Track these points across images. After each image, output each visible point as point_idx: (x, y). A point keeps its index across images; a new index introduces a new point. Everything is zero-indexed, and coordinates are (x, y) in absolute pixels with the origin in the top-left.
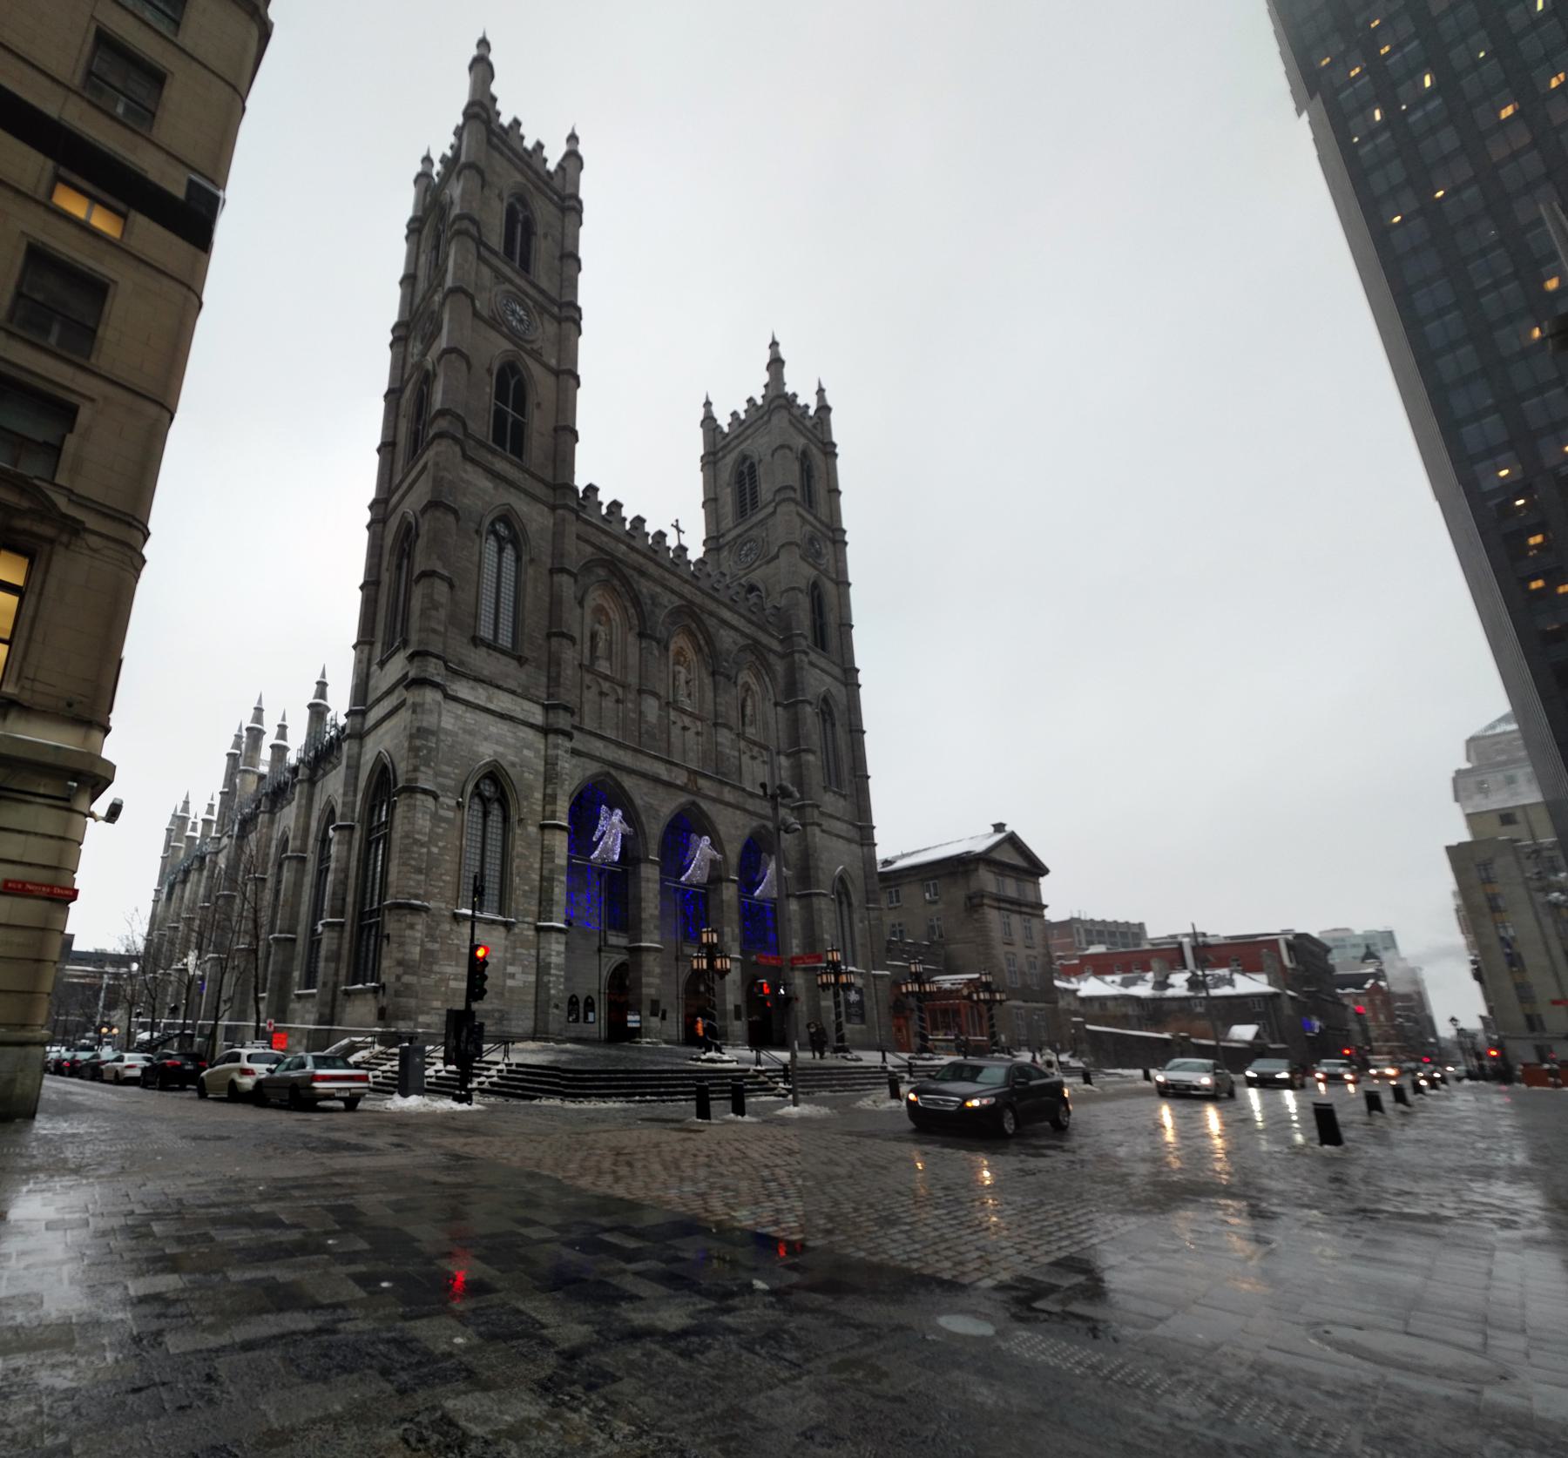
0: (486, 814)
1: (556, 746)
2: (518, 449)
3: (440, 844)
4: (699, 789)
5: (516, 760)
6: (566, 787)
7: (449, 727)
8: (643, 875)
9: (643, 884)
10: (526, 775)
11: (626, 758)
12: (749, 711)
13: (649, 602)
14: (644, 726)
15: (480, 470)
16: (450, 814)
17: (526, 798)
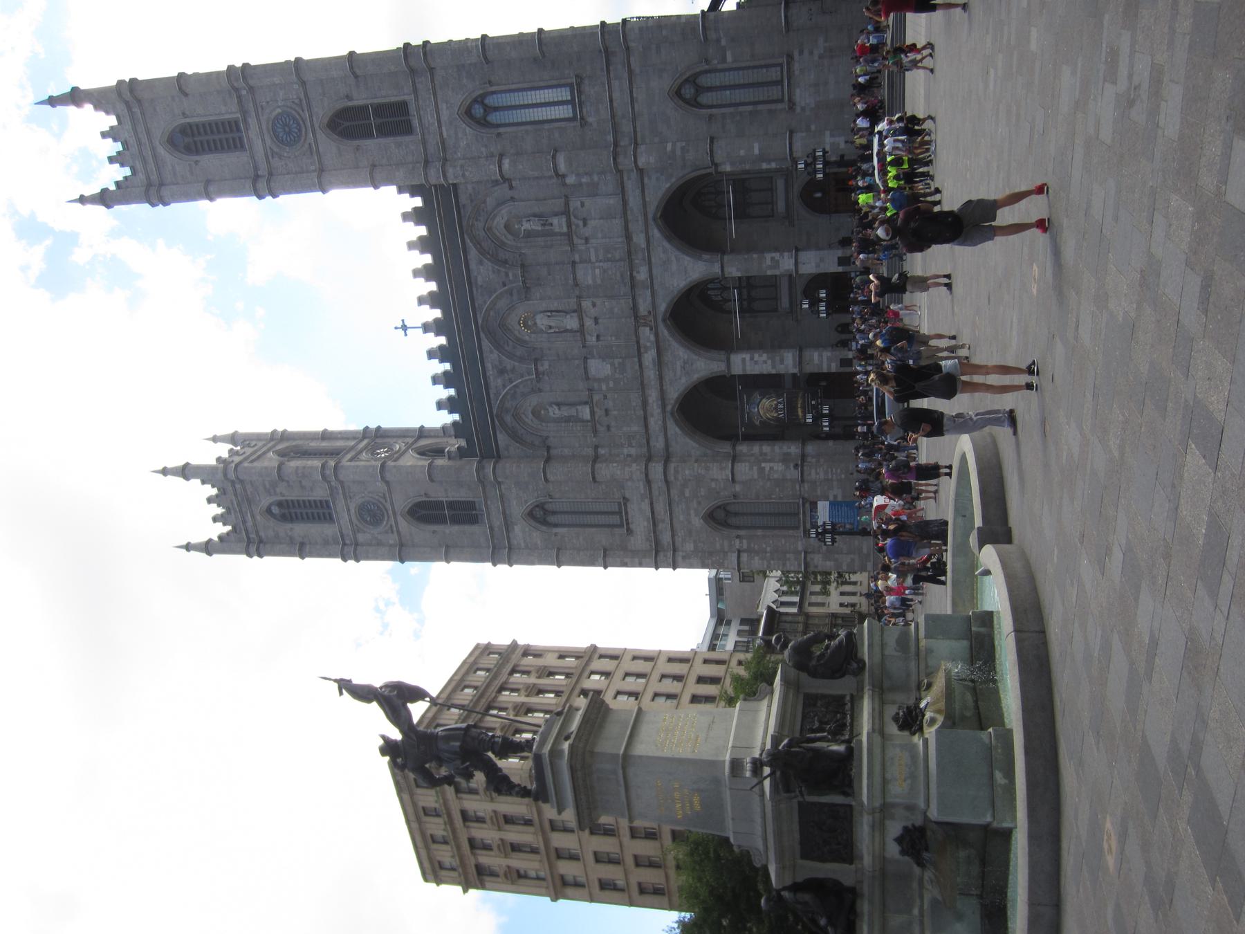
0: (736, 514)
1: (676, 479)
2: (471, 505)
3: (764, 546)
4: (649, 312)
5: (695, 501)
6: (703, 472)
7: (692, 545)
8: (741, 373)
9: (748, 373)
10: (703, 494)
11: (653, 396)
12: (535, 226)
13: (506, 377)
14: (617, 376)
15: (511, 535)
16: (745, 541)
17: (718, 493)
